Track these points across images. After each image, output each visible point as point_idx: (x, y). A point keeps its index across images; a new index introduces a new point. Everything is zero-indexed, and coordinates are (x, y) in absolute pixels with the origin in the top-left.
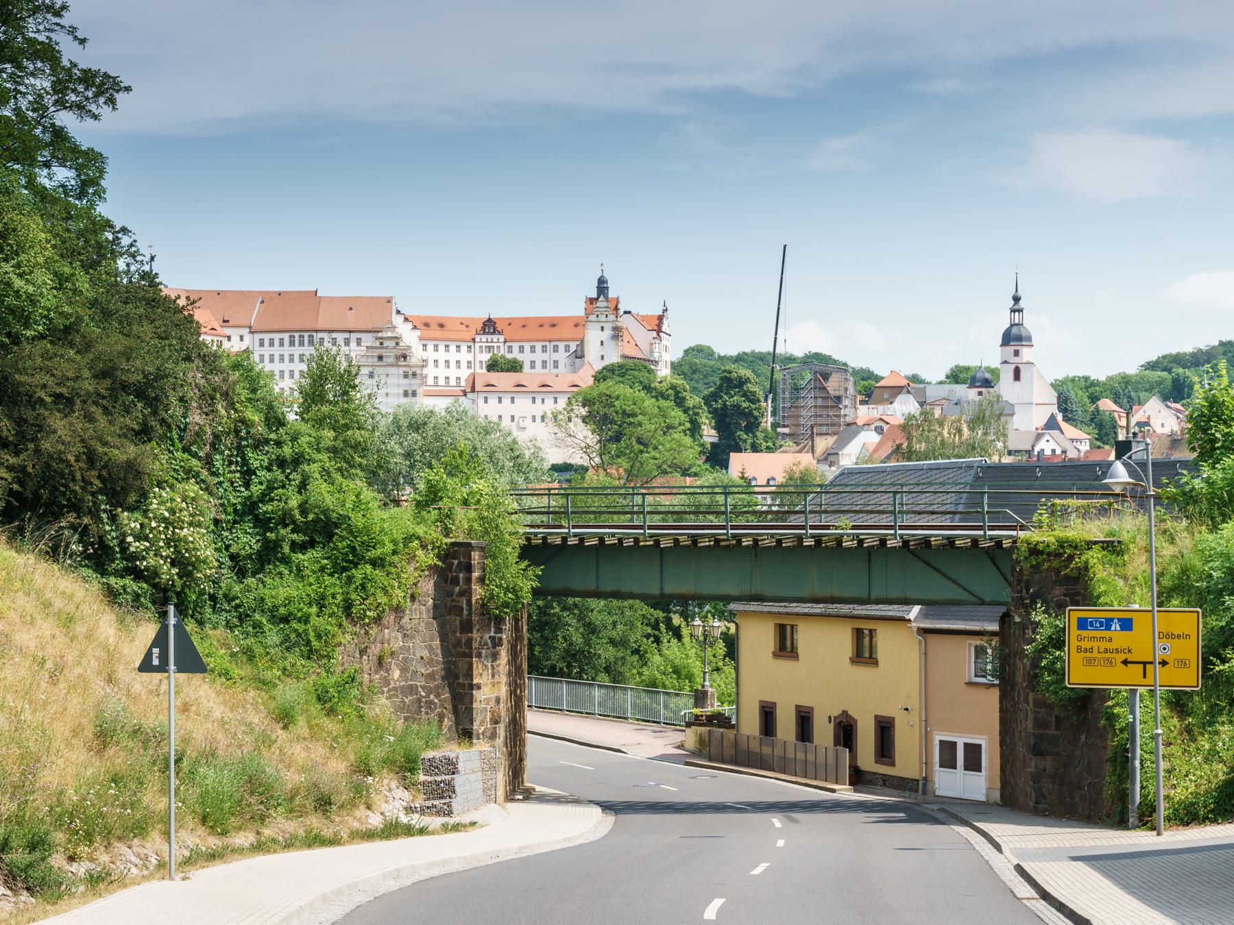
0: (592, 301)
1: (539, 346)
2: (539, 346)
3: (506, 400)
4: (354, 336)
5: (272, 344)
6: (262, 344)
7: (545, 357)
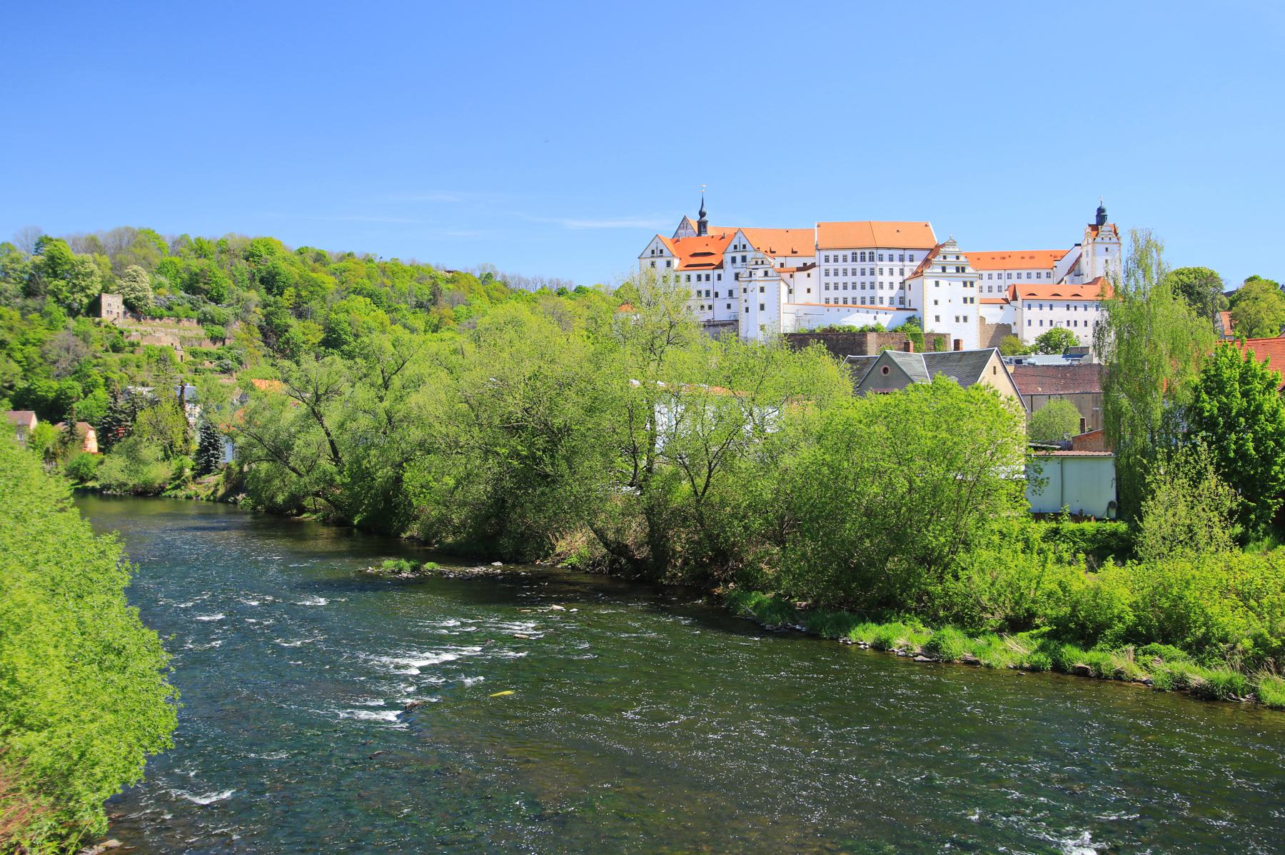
0: (1095, 228)
1: (995, 274)
2: (995, 274)
3: (1046, 309)
4: (907, 253)
5: (836, 260)
6: (827, 260)
7: (1001, 282)
